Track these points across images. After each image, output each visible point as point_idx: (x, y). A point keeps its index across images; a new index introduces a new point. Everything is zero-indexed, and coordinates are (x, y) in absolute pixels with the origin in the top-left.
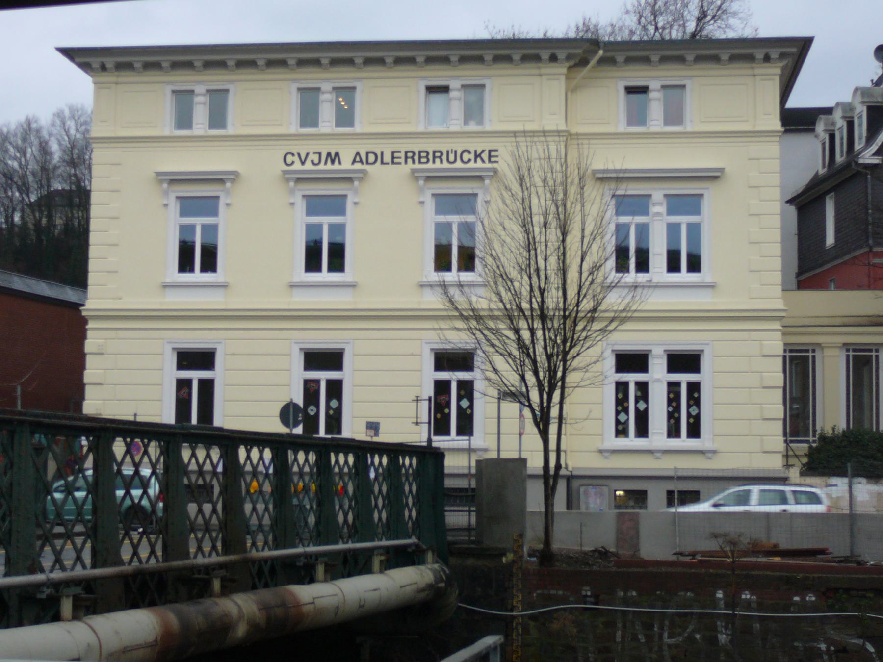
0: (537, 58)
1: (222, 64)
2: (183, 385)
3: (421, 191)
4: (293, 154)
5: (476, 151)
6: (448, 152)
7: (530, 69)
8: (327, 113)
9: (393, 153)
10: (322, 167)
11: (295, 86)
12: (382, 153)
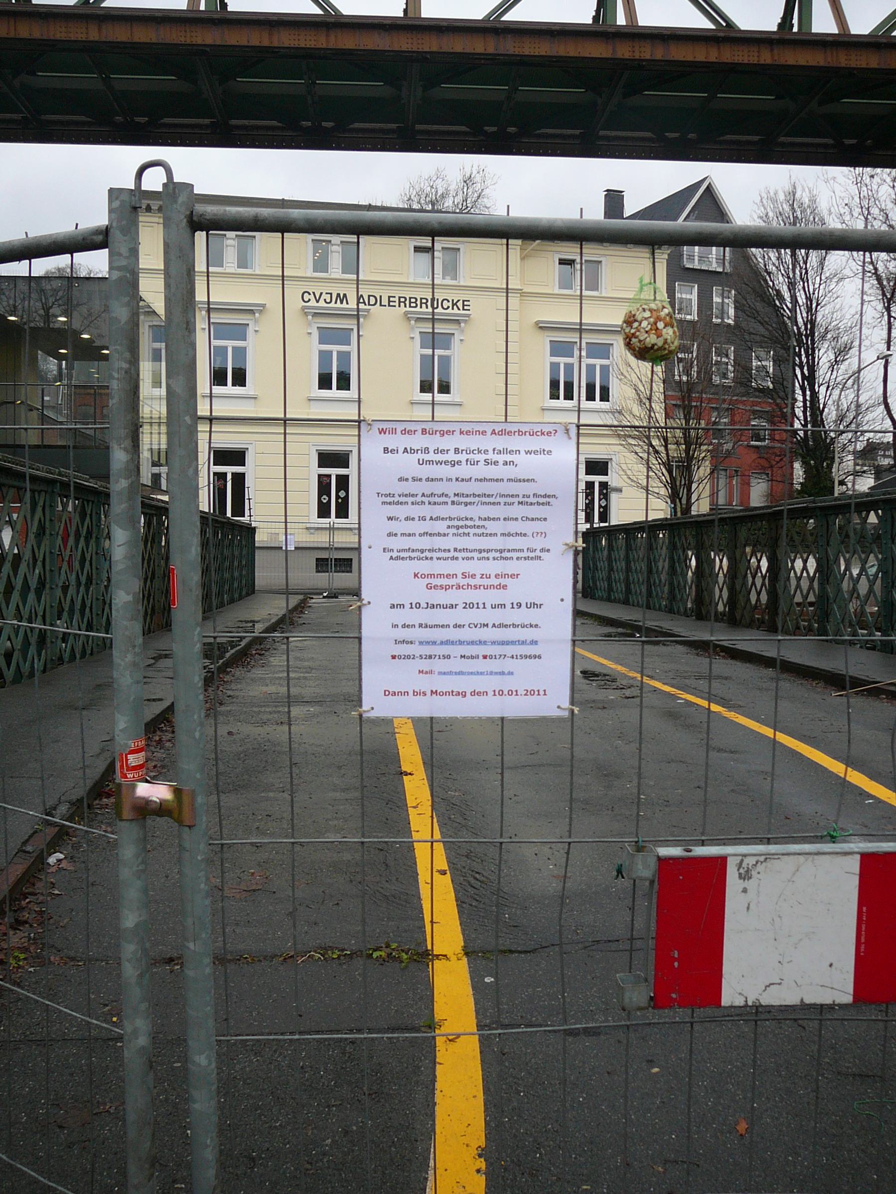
3: (310, 324)
5: (453, 300)
9: (389, 297)
10: (332, 305)
12: (381, 297)
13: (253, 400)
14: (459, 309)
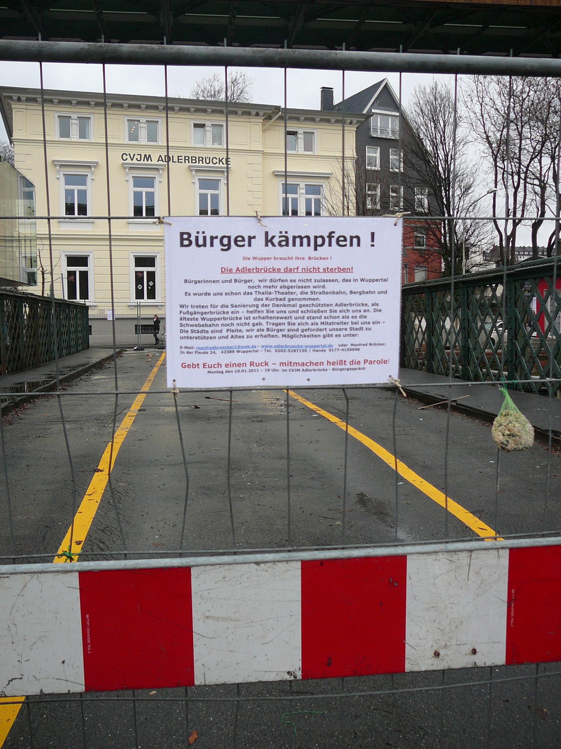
0: (249, 114)
1: (88, 104)
2: (71, 274)
3: (127, 175)
4: (127, 155)
5: (219, 158)
6: (206, 158)
7: (245, 119)
8: (74, 130)
9: (178, 157)
10: (142, 162)
11: (126, 118)
12: (173, 156)
13: (92, 224)
14: (223, 164)
